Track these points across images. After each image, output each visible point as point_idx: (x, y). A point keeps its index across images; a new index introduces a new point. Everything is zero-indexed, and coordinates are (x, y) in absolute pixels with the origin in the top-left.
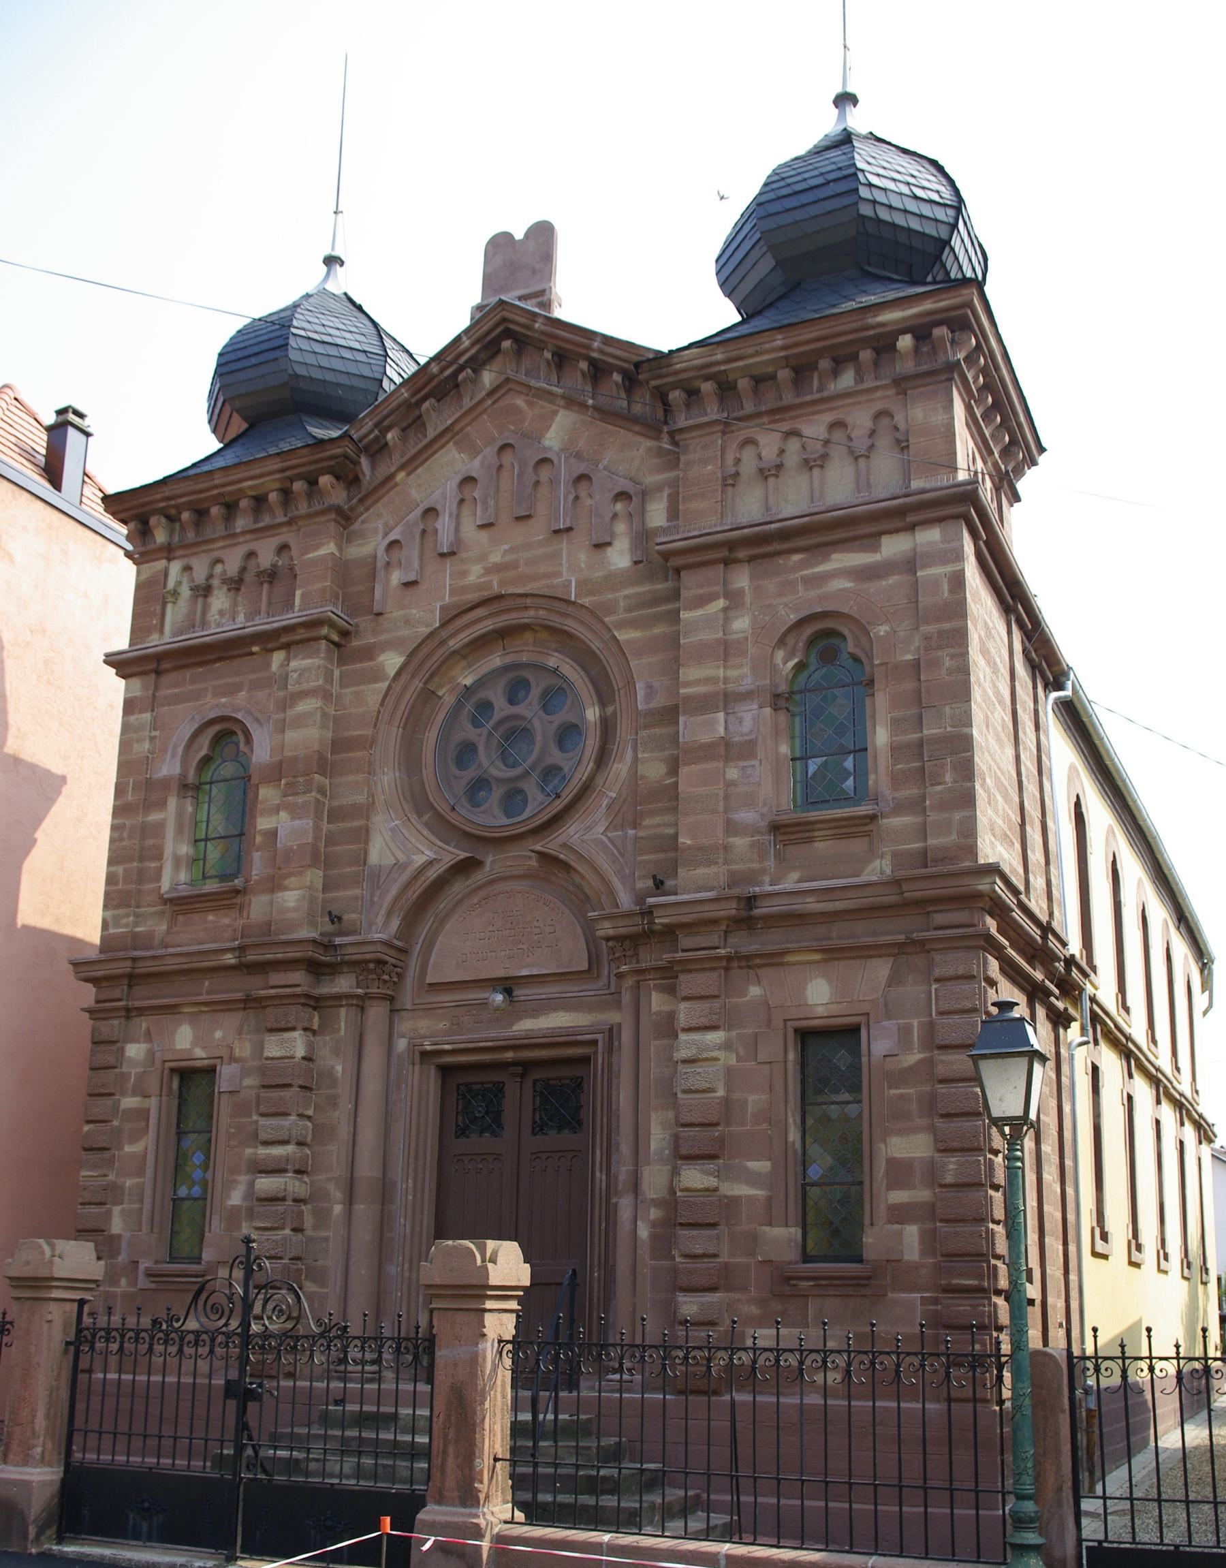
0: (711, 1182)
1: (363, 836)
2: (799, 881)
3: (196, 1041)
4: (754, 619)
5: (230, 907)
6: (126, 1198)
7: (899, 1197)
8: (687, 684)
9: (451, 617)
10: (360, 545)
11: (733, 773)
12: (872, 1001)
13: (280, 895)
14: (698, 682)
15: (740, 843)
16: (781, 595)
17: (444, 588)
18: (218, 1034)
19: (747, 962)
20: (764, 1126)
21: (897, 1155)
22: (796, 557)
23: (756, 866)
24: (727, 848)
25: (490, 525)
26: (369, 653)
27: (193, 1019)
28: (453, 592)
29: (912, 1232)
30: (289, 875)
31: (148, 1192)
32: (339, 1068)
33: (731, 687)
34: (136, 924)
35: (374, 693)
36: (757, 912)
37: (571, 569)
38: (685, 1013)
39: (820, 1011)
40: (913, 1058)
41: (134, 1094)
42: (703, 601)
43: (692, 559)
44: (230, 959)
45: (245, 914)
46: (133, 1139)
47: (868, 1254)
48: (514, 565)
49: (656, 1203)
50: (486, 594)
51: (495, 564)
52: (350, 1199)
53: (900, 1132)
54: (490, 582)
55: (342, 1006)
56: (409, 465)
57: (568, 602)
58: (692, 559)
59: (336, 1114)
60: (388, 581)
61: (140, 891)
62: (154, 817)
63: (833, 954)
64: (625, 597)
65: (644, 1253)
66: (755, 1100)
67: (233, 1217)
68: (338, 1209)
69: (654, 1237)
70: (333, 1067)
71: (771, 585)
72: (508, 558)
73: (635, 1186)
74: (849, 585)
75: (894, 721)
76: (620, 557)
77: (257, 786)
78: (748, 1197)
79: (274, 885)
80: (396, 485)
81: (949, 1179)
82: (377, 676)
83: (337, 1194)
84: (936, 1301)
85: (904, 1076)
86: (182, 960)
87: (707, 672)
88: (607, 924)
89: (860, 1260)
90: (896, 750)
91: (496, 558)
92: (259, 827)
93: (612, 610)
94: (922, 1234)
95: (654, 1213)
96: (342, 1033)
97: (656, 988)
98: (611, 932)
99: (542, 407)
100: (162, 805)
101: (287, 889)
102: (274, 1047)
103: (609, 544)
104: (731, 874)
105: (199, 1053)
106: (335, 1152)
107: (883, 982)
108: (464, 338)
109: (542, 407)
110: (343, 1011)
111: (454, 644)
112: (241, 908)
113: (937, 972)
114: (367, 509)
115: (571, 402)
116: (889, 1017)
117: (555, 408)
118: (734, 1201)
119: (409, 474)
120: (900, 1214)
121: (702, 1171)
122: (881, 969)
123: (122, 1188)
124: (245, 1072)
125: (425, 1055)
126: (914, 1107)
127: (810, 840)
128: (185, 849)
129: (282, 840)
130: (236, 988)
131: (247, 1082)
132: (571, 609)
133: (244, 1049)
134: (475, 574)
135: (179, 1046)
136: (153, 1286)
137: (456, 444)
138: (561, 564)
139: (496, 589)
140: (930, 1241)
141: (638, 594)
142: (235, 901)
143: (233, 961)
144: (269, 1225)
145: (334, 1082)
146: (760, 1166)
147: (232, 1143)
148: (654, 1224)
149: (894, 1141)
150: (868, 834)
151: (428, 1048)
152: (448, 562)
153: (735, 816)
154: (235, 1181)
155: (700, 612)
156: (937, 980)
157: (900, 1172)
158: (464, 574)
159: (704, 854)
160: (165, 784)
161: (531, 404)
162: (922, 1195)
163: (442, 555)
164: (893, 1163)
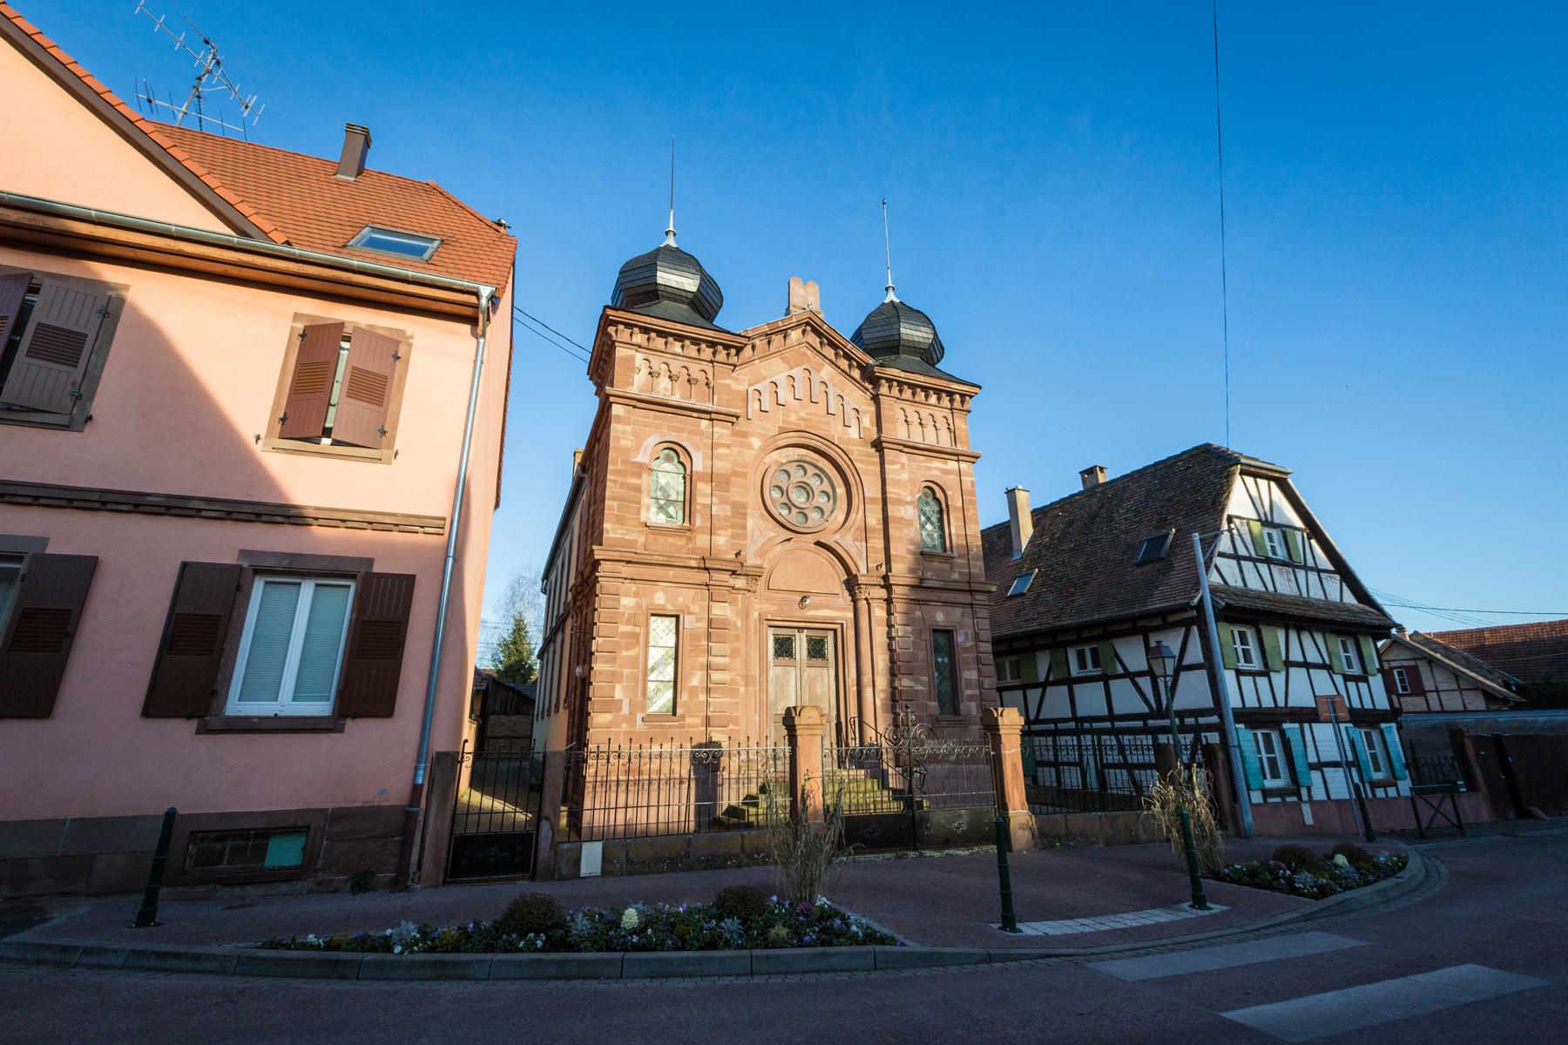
3: (667, 600)
9: (783, 431)
40: (969, 644)
41: (628, 623)
44: (693, 563)
85: (967, 650)
91: (802, 414)
105: (669, 607)
122: (958, 611)
124: (698, 620)
133: (695, 608)
134: (793, 418)
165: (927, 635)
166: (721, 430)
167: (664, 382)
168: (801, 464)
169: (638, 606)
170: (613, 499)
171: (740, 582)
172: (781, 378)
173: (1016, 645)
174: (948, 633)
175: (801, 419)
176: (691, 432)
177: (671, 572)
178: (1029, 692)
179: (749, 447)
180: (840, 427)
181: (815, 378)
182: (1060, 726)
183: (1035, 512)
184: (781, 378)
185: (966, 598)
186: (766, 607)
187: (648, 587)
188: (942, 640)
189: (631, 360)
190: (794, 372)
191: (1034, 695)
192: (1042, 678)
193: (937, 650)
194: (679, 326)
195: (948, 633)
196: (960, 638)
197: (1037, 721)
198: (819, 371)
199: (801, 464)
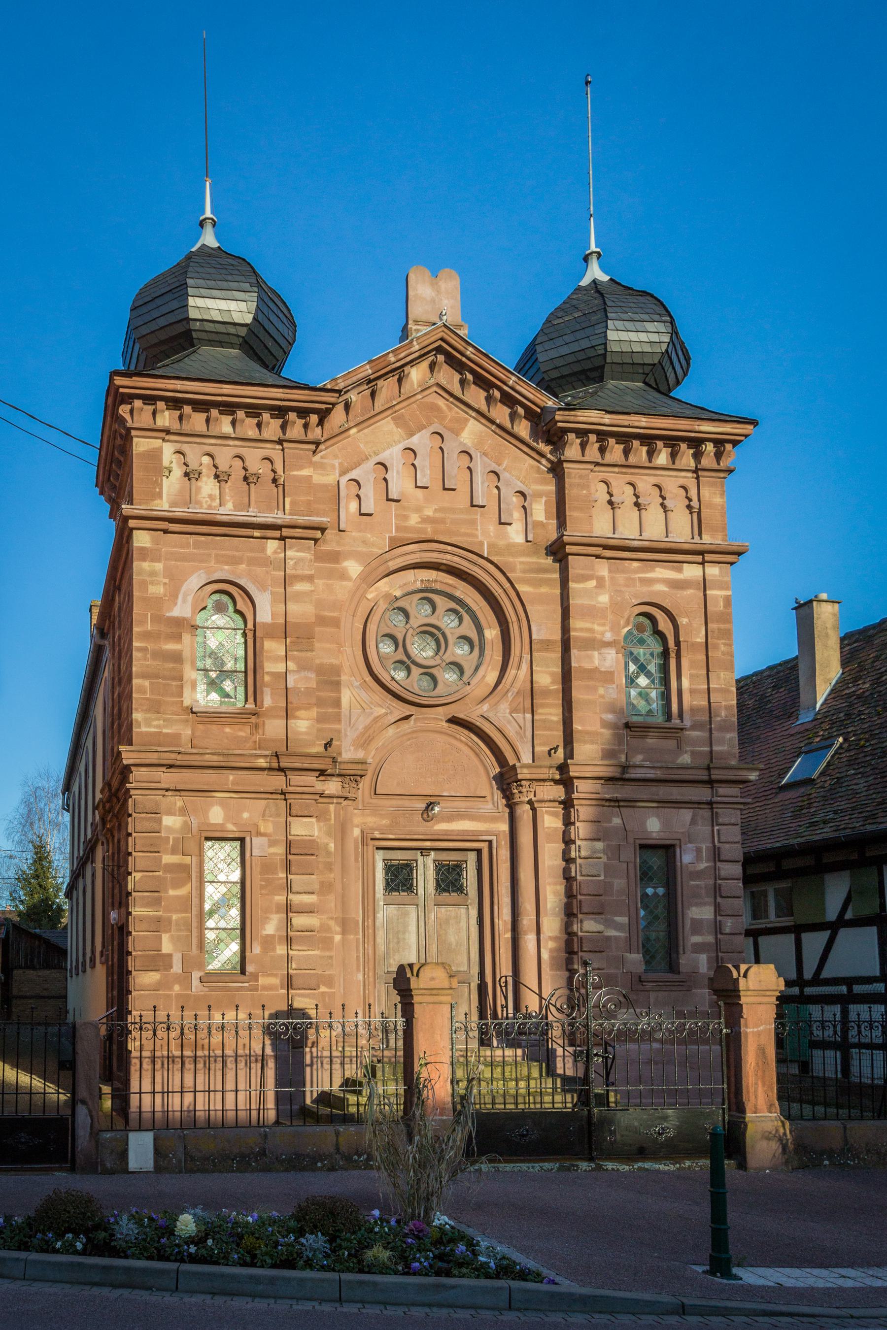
2: (643, 761)
3: (227, 818)
4: (611, 597)
5: (244, 724)
6: (173, 928)
7: (696, 939)
10: (323, 475)
12: (683, 833)
14: (581, 630)
16: (627, 586)
17: (390, 523)
18: (246, 815)
21: (695, 917)
22: (635, 564)
29: (703, 958)
33: (598, 636)
34: (165, 727)
37: (484, 534)
39: (654, 835)
40: (703, 865)
41: (174, 852)
42: (584, 578)
45: (260, 731)
46: (177, 885)
47: (682, 969)
48: (443, 521)
51: (428, 517)
53: (697, 905)
54: (426, 528)
71: (621, 578)
74: (666, 589)
75: (692, 676)
76: (515, 534)
78: (615, 937)
85: (697, 875)
87: (588, 625)
89: (679, 973)
92: (266, 670)
94: (709, 959)
105: (230, 827)
109: (457, 413)
114: (326, 448)
116: (690, 842)
118: (608, 938)
119: (359, 431)
120: (699, 948)
122: (686, 815)
123: (170, 921)
124: (272, 843)
126: (703, 892)
127: (645, 737)
131: (273, 850)
133: (267, 827)
135: (212, 821)
137: (393, 419)
141: (529, 563)
147: (263, 892)
161: (450, 409)
165: (629, 854)
166: (298, 555)
167: (208, 486)
168: (427, 595)
169: (186, 827)
170: (144, 676)
171: (332, 787)
172: (393, 454)
173: (788, 864)
174: (667, 850)
175: (426, 520)
176: (252, 562)
177: (231, 777)
178: (806, 937)
179: (343, 576)
180: (492, 527)
181: (452, 446)
182: (858, 989)
183: (845, 640)
184: (393, 454)
185: (703, 793)
186: (371, 821)
188: (656, 861)
189: (155, 456)
190: (415, 441)
191: (814, 942)
192: (832, 914)
193: (646, 876)
194: (227, 389)
195: (667, 850)
196: (686, 857)
197: (816, 980)
198: (457, 433)
199: (427, 595)
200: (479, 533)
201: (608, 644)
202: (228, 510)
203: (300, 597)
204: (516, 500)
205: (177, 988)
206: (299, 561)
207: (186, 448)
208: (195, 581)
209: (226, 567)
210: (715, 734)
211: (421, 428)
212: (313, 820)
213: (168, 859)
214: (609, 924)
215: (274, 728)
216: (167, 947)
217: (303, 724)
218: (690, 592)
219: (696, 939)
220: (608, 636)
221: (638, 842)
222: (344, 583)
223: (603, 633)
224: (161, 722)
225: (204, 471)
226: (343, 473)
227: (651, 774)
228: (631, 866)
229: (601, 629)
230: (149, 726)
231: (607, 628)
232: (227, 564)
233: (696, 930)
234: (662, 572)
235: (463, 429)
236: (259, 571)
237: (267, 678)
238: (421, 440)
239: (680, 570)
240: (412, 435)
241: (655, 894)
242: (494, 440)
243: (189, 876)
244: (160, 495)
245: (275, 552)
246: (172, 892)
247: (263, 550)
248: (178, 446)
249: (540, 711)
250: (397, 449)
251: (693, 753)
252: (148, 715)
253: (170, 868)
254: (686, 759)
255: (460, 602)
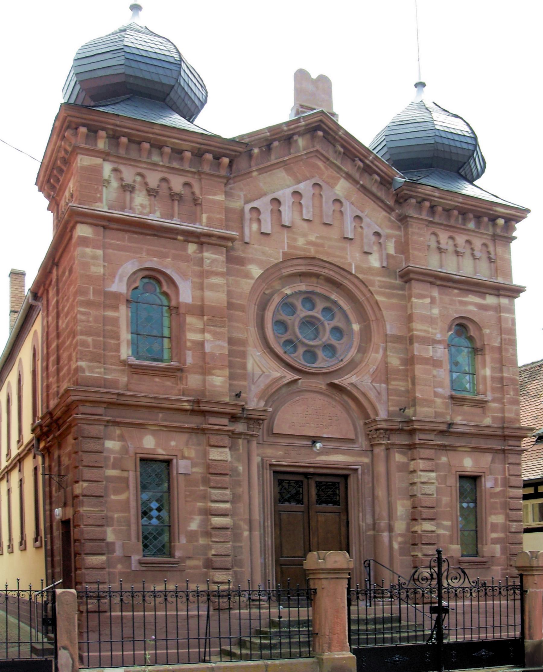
0: (433, 528)
1: (243, 355)
3: (158, 445)
4: (440, 311)
7: (494, 535)
8: (417, 330)
9: (288, 258)
11: (435, 372)
13: (209, 378)
14: (421, 330)
15: (439, 401)
16: (450, 304)
18: (173, 443)
19: (444, 448)
20: (448, 509)
22: (456, 291)
23: (444, 411)
24: (434, 402)
25: (310, 221)
26: (241, 261)
27: (154, 433)
28: (289, 246)
29: (498, 547)
30: (214, 368)
31: (133, 520)
32: (241, 468)
34: (105, 374)
35: (246, 285)
36: (452, 430)
37: (352, 259)
38: (422, 464)
39: (469, 469)
40: (498, 489)
41: (114, 468)
42: (422, 296)
43: (421, 278)
44: (186, 406)
45: (184, 382)
46: (117, 492)
49: (400, 535)
50: (308, 254)
52: (251, 530)
53: (495, 514)
55: (240, 438)
56: (261, 171)
57: (351, 273)
58: (421, 278)
59: (241, 490)
60: (250, 228)
61: (105, 355)
62: (110, 313)
63: (475, 449)
64: (379, 281)
65: (396, 554)
66: (445, 500)
67: (192, 536)
68: (246, 533)
69: (400, 548)
70: (237, 467)
71: (446, 299)
72: (319, 241)
73: (390, 529)
74: (475, 309)
77: (184, 314)
79: (205, 369)
80: (251, 177)
81: (513, 530)
82: (247, 275)
83: (246, 527)
84: (506, 569)
85: (495, 495)
86: (153, 401)
87: (425, 328)
88: (383, 423)
90: (493, 378)
91: (312, 238)
93: (373, 285)
95: (400, 539)
96: (241, 451)
97: (397, 452)
98: (385, 427)
99: (332, 172)
100: (116, 308)
101: (214, 375)
102: (215, 454)
103: (371, 253)
104: (436, 412)
105: (160, 451)
106: (242, 507)
107: (490, 462)
108: (302, 120)
110: (240, 441)
111: (286, 272)
112: (181, 379)
113: (510, 461)
115: (349, 177)
116: (491, 474)
117: (338, 175)
118: (438, 535)
120: (495, 541)
121: (431, 524)
122: (488, 457)
123: (112, 518)
124: (194, 465)
125: (271, 465)
126: (499, 506)
128: (129, 337)
129: (208, 348)
130: (195, 421)
131: (194, 470)
132: (349, 276)
134: (301, 242)
136: (144, 569)
138: (347, 254)
139: (312, 253)
140: (504, 550)
141: (383, 282)
142: (176, 374)
143: (188, 407)
144: (222, 540)
145: (238, 474)
146: (447, 523)
147: (188, 499)
148: (400, 543)
149: (493, 517)
150: (483, 408)
151: (275, 463)
152: (285, 231)
153: (436, 390)
154: (192, 518)
155: (421, 301)
156: (509, 464)
157: (494, 527)
158: (295, 240)
159: (428, 403)
160: (116, 296)
162: (502, 535)
163: (283, 226)
164: (493, 525)
165: (453, 481)
169: (125, 450)
171: (240, 427)
172: (285, 195)
181: (328, 195)
184: (285, 195)
187: (135, 432)
188: (468, 485)
190: (301, 187)
193: (462, 495)
196: (488, 483)
198: (332, 186)
200: (349, 257)
201: (439, 342)
202: (155, 218)
203: (214, 287)
204: (373, 238)
205: (119, 566)
206: (213, 261)
207: (122, 168)
208: (129, 267)
209: (155, 259)
210: (507, 406)
211: (306, 179)
212: (227, 450)
213: (111, 473)
214: (438, 526)
215: (193, 381)
216: (110, 537)
217: (218, 381)
218: (491, 313)
219: (494, 535)
220: (439, 337)
221: (458, 473)
222: (248, 281)
223: (435, 334)
224: (102, 370)
225: (137, 186)
226: (247, 202)
227: (467, 430)
228: (454, 488)
229: (434, 331)
230: (93, 372)
231: (438, 331)
232: (155, 256)
233: (493, 531)
234: (472, 298)
235: (336, 184)
236: (183, 265)
237: (189, 344)
238: (304, 187)
239: (484, 298)
240: (299, 182)
241: (468, 507)
242: (357, 196)
243: (128, 487)
244: (100, 200)
245: (195, 252)
246: (113, 497)
247: (185, 249)
248: (116, 166)
249: (393, 383)
250: (289, 191)
251: (493, 418)
252: (91, 364)
253: (109, 479)
254: (488, 421)
255: (335, 303)
